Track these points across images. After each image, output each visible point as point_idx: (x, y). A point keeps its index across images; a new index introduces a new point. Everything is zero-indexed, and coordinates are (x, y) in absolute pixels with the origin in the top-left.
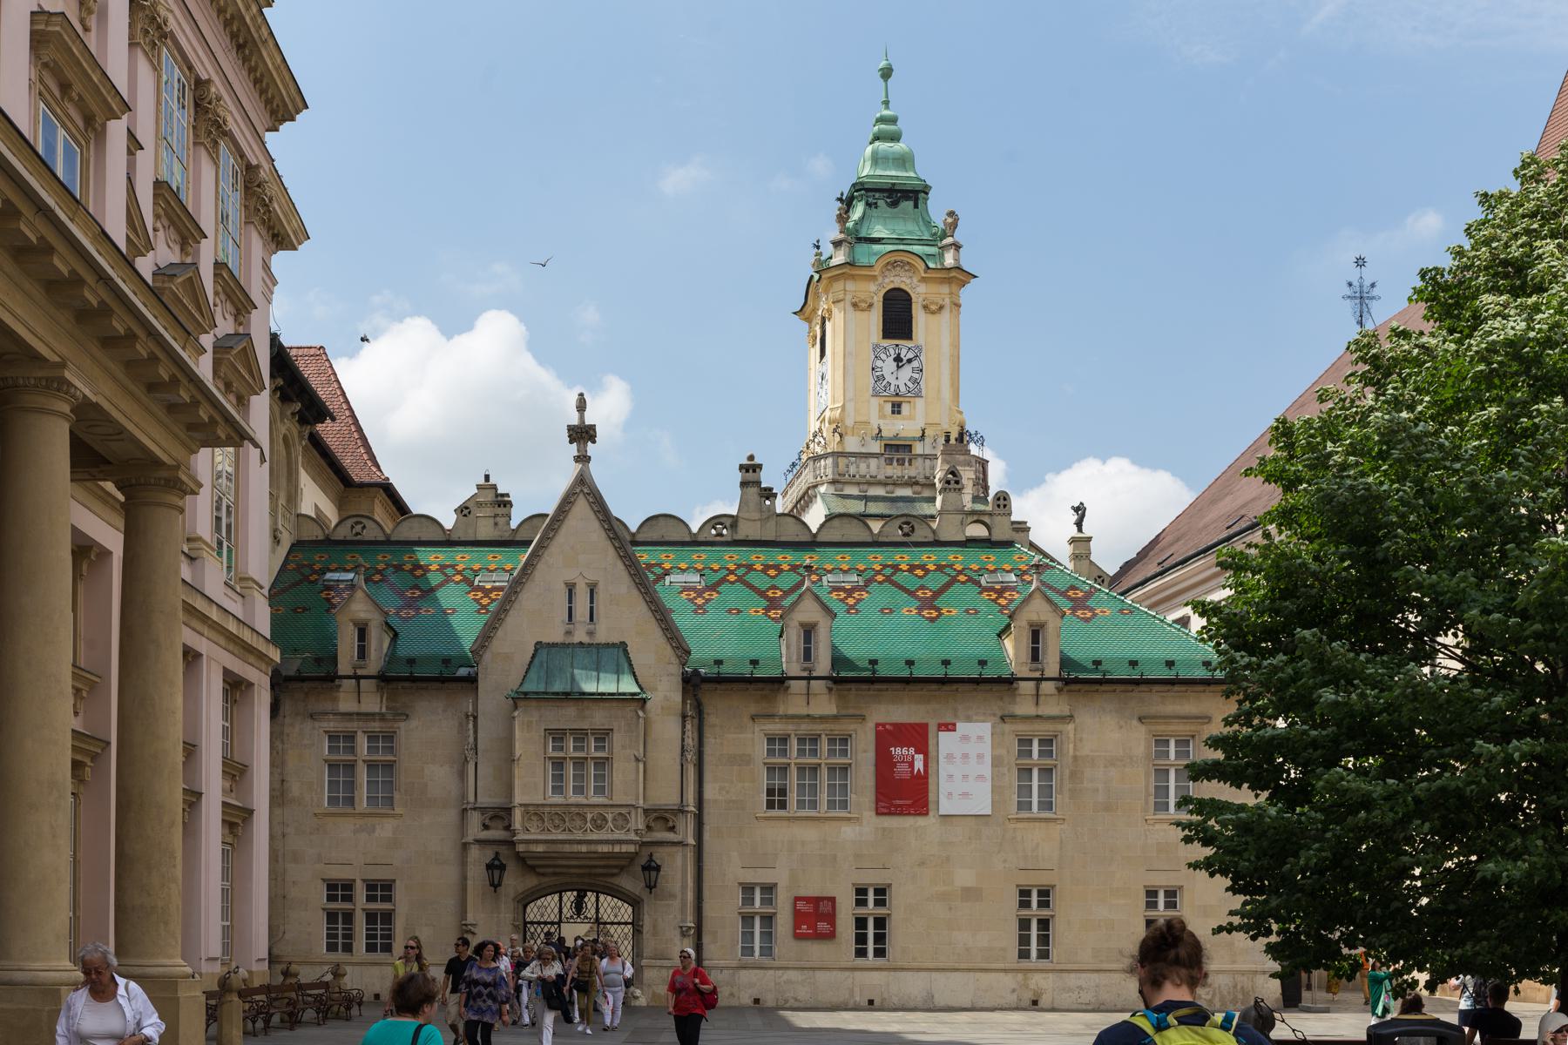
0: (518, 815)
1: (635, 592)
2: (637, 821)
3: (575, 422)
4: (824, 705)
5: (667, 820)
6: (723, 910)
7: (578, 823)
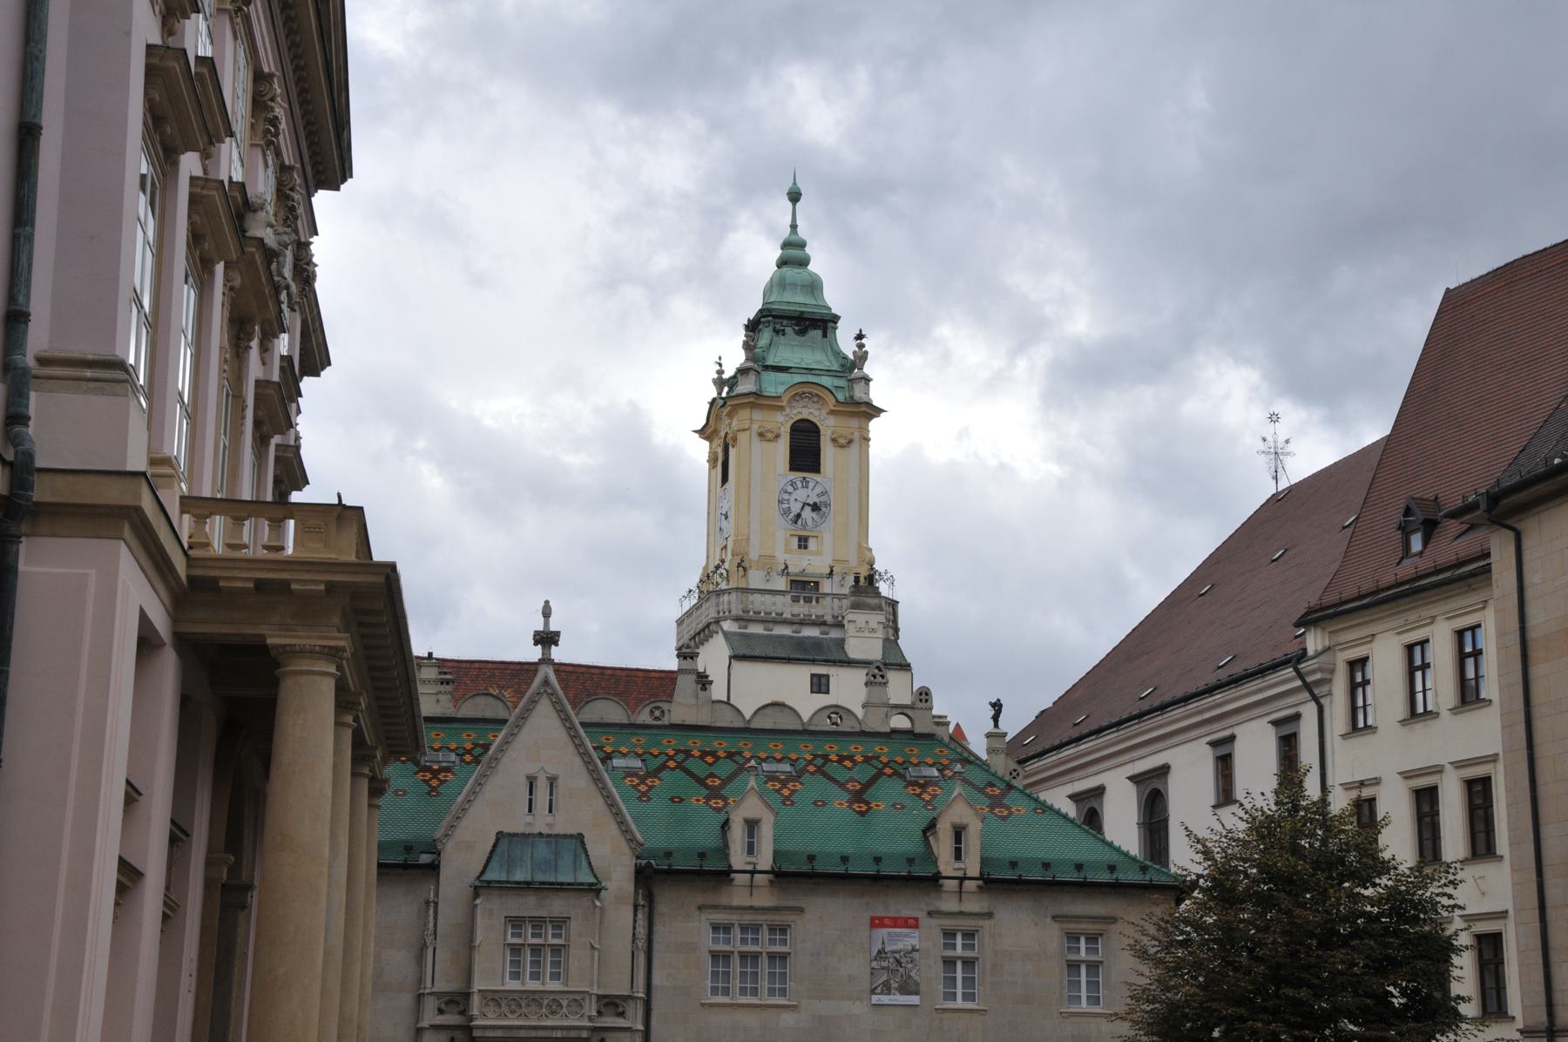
0: (476, 1000)
1: (593, 787)
2: (591, 1008)
3: (541, 628)
4: (764, 899)
5: (617, 1006)
7: (534, 1008)
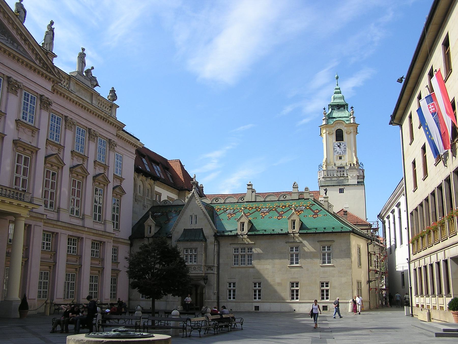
6: (224, 288)
